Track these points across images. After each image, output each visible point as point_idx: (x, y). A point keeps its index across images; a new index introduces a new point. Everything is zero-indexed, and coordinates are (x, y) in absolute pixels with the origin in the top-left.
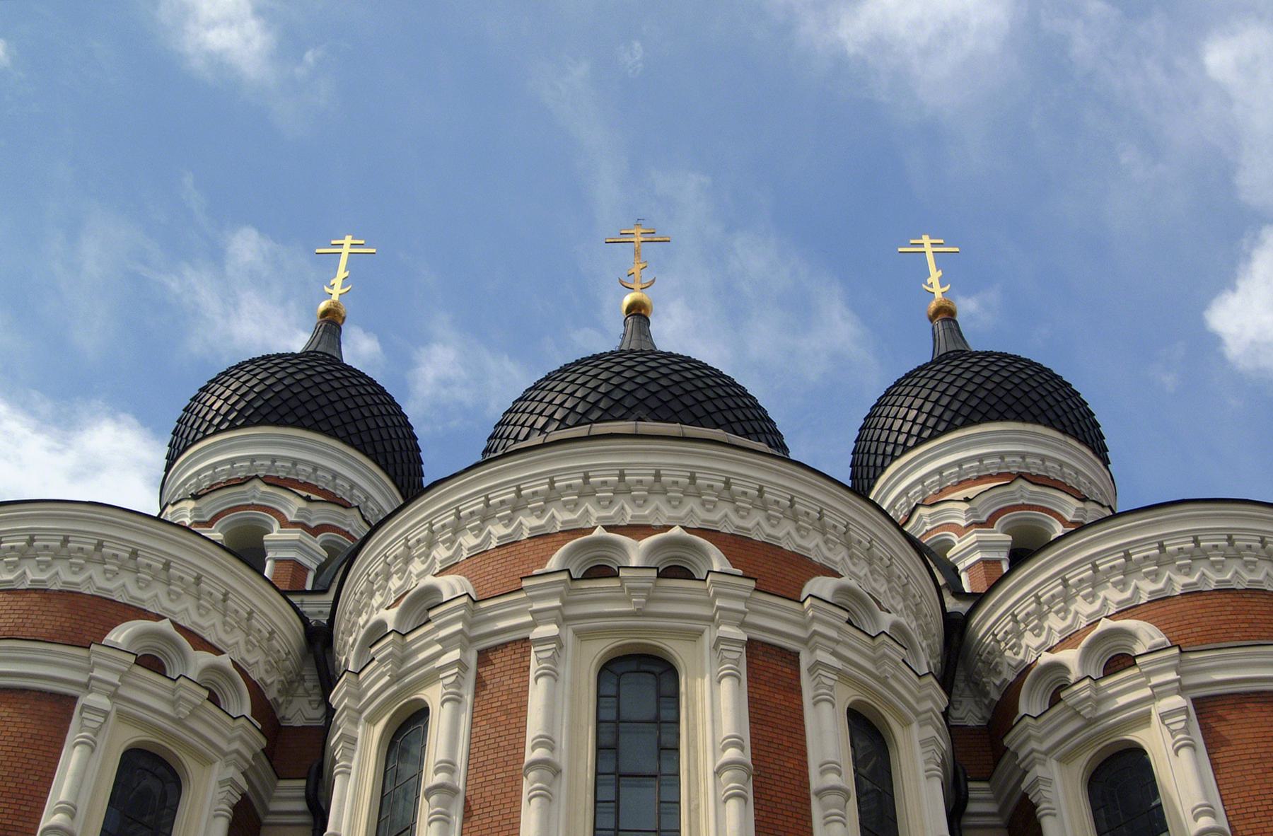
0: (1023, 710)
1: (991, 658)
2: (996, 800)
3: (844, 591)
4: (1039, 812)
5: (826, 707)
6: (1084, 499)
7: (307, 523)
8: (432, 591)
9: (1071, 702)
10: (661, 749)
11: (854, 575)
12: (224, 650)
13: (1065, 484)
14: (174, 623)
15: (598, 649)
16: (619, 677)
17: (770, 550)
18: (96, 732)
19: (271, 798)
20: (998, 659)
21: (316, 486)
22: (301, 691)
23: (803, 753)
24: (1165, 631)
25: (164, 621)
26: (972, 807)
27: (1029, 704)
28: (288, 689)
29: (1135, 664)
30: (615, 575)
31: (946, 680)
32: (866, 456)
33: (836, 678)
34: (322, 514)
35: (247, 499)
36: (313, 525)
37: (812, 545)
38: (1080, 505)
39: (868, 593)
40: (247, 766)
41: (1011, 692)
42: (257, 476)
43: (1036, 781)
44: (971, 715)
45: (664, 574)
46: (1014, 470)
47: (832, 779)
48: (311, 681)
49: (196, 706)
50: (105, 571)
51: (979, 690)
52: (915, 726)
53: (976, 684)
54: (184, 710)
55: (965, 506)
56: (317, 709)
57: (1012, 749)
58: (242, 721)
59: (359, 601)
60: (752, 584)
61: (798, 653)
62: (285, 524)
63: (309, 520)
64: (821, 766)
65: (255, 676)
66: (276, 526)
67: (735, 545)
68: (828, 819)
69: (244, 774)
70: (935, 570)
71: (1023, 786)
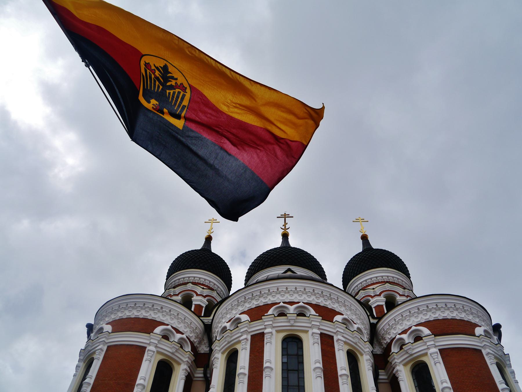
0: (393, 351)
2: (386, 375)
3: (345, 319)
4: (399, 379)
5: (341, 351)
6: (405, 288)
7: (203, 294)
8: (239, 319)
9: (405, 349)
11: (347, 315)
13: (399, 284)
14: (171, 326)
15: (282, 335)
17: (325, 308)
20: (385, 336)
21: (205, 285)
22: (203, 343)
24: (430, 330)
26: (380, 377)
27: (394, 349)
28: (200, 343)
29: (422, 339)
30: (286, 315)
31: (371, 342)
32: (346, 276)
33: (343, 343)
34: (206, 292)
35: (187, 288)
36: (204, 295)
37: (336, 307)
38: (403, 290)
39: (351, 319)
40: (190, 365)
41: (389, 345)
42: (190, 282)
43: (397, 371)
44: (378, 351)
45: (299, 315)
47: (344, 372)
48: (206, 341)
49: (177, 349)
50: (154, 313)
51: (380, 344)
52: (364, 356)
56: (207, 348)
57: (390, 361)
58: (189, 353)
59: (219, 320)
60: (321, 318)
62: (197, 295)
63: (203, 294)
64: (341, 368)
65: (192, 340)
66: (195, 295)
67: (317, 307)
69: (189, 367)
70: (367, 311)
71: (394, 372)
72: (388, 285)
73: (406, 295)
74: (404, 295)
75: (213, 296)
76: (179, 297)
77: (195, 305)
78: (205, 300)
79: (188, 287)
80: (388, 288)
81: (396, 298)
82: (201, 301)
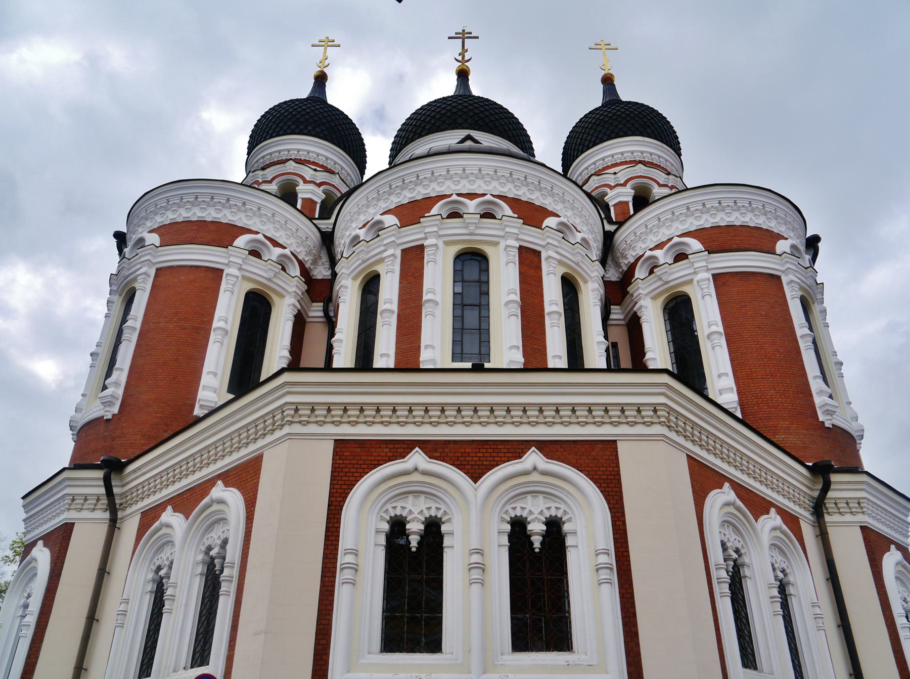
0: (636, 276)
1: (624, 252)
2: (623, 313)
3: (562, 224)
5: (552, 276)
6: (669, 174)
7: (315, 181)
8: (379, 222)
9: (658, 274)
10: (481, 294)
11: (566, 216)
12: (286, 246)
13: (660, 166)
14: (264, 235)
15: (454, 250)
16: (463, 262)
17: (529, 205)
18: (234, 285)
19: (310, 310)
20: (626, 252)
21: (318, 163)
22: (320, 263)
23: (542, 296)
24: (702, 244)
25: (259, 234)
26: (612, 316)
27: (640, 273)
28: (315, 262)
29: (688, 258)
30: (461, 216)
31: (603, 262)
32: (569, 151)
33: (557, 263)
34: (321, 177)
35: (287, 170)
36: (318, 182)
37: (548, 203)
38: (666, 176)
39: (572, 224)
40: (299, 298)
41: (632, 267)
42: (291, 159)
43: (641, 307)
44: (613, 275)
46: (638, 159)
47: (554, 308)
48: (325, 258)
49: (276, 273)
50: (232, 212)
51: (617, 265)
53: (616, 263)
54: (271, 274)
55: (613, 176)
56: (328, 271)
57: (631, 293)
58: (297, 278)
59: (346, 224)
60: (521, 221)
61: (540, 252)
62: (305, 181)
63: (316, 180)
65: (300, 258)
66: (301, 182)
67: (515, 204)
68: (552, 325)
69: (298, 301)
70: (600, 211)
71: (635, 309)
72: (640, 167)
73: (670, 185)
74: (666, 186)
75: (333, 183)
76: (272, 185)
77: (303, 199)
78: (319, 191)
79: (288, 168)
80: (640, 172)
81: (651, 190)
82: (312, 192)
